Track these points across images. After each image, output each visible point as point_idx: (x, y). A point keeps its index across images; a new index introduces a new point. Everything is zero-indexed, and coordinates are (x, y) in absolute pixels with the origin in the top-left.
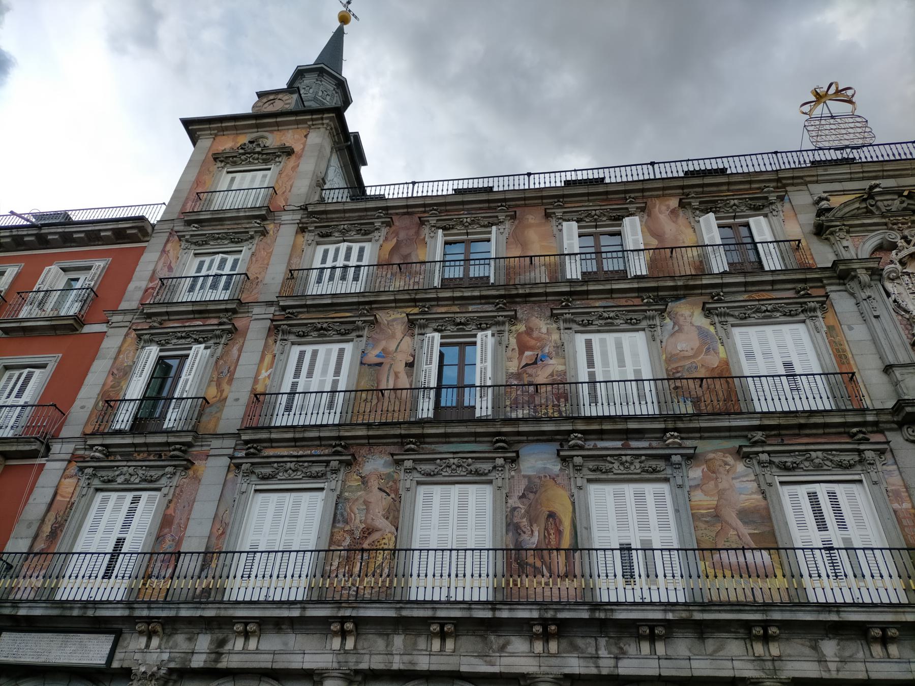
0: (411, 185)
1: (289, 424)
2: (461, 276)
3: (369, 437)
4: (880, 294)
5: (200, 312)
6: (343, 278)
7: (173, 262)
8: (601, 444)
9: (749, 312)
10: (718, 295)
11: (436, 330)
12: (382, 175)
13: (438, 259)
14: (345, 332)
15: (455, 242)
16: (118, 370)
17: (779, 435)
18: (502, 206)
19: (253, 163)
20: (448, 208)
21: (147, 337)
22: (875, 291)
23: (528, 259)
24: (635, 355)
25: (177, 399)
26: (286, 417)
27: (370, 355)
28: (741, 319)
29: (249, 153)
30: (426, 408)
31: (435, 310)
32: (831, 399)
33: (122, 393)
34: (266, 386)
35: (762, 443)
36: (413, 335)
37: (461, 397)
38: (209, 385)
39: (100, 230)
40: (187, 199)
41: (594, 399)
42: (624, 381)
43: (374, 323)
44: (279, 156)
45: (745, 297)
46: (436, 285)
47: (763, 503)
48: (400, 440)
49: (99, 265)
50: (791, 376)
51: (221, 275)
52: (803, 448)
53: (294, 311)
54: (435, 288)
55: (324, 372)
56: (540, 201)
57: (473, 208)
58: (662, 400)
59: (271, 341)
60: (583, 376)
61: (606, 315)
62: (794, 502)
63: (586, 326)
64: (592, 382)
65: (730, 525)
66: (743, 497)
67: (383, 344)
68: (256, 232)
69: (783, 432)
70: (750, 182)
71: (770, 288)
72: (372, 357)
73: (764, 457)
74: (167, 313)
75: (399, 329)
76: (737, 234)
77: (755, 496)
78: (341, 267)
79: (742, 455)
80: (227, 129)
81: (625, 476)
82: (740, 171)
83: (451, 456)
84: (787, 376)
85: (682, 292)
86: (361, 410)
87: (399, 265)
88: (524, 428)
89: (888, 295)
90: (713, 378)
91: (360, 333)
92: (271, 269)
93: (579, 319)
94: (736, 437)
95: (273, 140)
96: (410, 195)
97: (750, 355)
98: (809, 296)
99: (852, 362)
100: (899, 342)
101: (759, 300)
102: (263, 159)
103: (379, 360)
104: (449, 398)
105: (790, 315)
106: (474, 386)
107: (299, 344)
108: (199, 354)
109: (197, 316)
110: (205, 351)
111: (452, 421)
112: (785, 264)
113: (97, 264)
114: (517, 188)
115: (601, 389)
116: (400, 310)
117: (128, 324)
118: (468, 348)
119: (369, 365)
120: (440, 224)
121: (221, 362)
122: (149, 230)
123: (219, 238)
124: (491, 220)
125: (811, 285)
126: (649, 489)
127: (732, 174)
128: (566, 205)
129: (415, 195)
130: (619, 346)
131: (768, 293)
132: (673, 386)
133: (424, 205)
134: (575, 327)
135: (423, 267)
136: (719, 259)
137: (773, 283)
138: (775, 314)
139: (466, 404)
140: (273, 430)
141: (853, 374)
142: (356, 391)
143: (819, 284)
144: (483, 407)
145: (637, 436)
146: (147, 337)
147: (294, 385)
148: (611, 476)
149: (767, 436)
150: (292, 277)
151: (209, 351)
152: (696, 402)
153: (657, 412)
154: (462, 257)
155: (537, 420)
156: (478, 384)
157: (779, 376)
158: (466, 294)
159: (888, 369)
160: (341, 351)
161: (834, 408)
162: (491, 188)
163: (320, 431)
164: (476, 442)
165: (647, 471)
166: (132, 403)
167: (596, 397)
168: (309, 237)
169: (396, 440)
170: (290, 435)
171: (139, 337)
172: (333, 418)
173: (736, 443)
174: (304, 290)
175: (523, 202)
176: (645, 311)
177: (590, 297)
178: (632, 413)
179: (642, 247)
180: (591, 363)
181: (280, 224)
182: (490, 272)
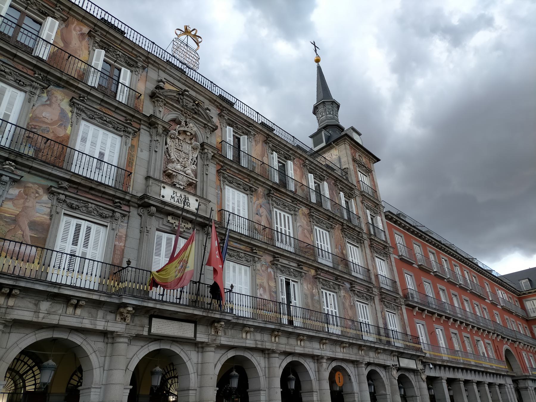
9: (96, 116)
17: (77, 188)
22: (161, 139)
28: (90, 118)
32: (114, 181)
35: (65, 189)
45: (98, 107)
47: (48, 221)
52: (86, 200)
62: (66, 227)
66: (38, 214)
69: (80, 188)
70: (133, 49)
73: (62, 197)
76: (112, 71)
77: (45, 216)
79: (50, 191)
82: (131, 39)
85: (63, 84)
89: (166, 144)
90: (55, 142)
97: (84, 140)
99: (134, 167)
100: (159, 168)
101: (104, 113)
127: (126, 37)
131: (111, 112)
136: (95, 78)
138: (109, 124)
149: (70, 187)
152: (38, 151)
157: (94, 158)
173: (49, 183)
176: (33, 81)
179: (52, 42)
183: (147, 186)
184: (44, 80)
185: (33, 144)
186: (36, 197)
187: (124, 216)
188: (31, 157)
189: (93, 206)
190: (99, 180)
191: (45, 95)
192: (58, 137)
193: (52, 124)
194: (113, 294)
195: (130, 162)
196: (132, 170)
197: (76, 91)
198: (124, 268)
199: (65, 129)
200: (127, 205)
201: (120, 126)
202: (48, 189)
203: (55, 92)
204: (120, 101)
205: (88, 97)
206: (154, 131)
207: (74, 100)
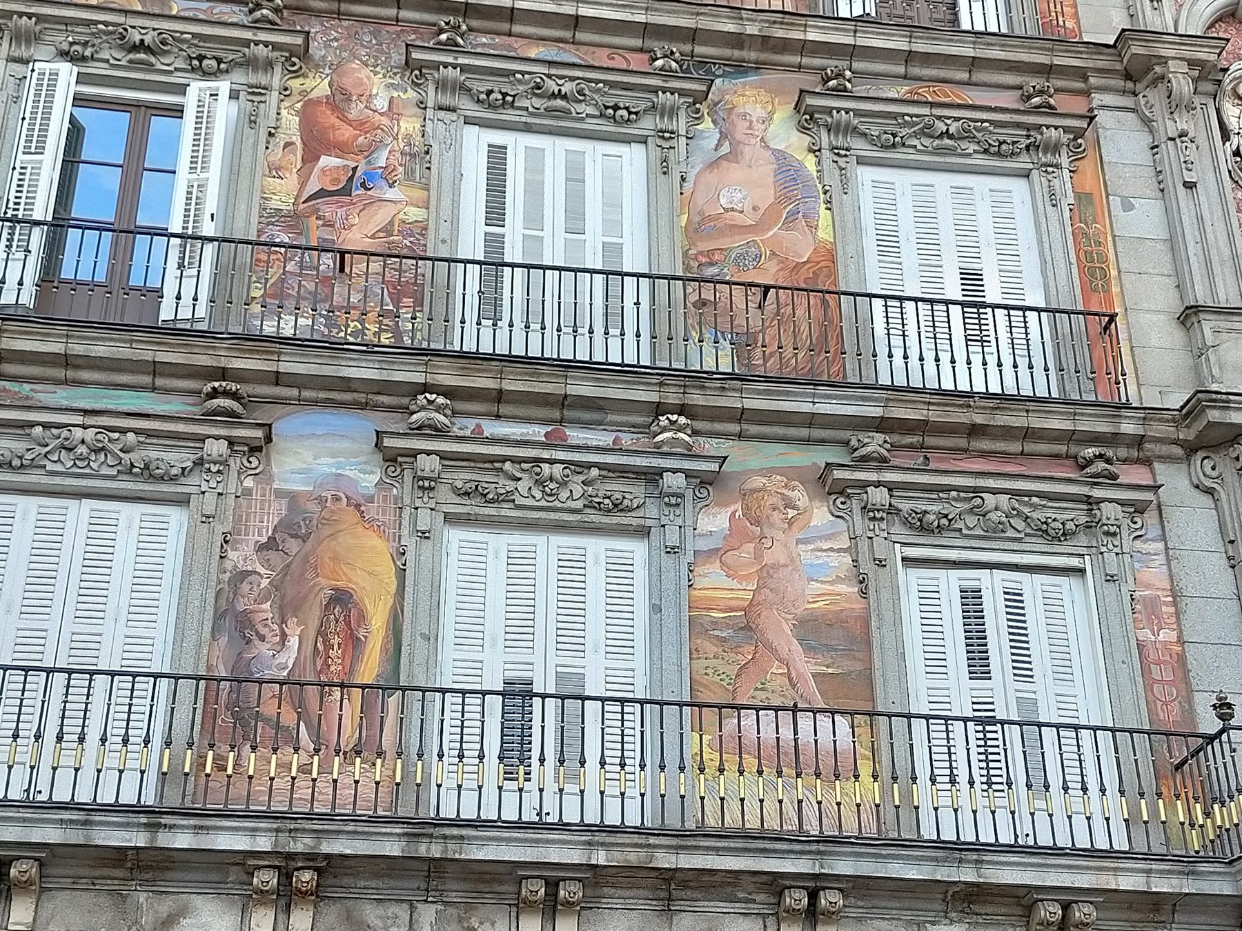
4: (1208, 130)
8: (492, 428)
9: (905, 131)
10: (840, 75)
11: (64, 55)
24: (612, 204)
37: (121, 260)
41: (491, 306)
42: (576, 270)
45: (902, 91)
50: (974, 305)
58: (663, 330)
60: (472, 245)
61: (551, 86)
63: (496, 108)
64: (493, 264)
65: (774, 652)
69: (931, 441)
71: (964, 76)
73: (879, 496)
77: (841, 588)
81: (543, 515)
84: (962, 304)
93: (479, 86)
94: (823, 442)
97: (889, 244)
98: (1050, 110)
101: (932, 105)
104: (85, 258)
105: (998, 154)
111: (88, 324)
112: (1010, 20)
115: (513, 283)
125: (1060, 84)
126: (596, 548)
130: (575, 177)
132: (694, 298)
134: (467, 106)
137: (974, 63)
139: (136, 280)
141: (1112, 318)
143: (1080, 85)
144: (185, 294)
145: (586, 416)
148: (507, 511)
149: (895, 447)
153: (645, 361)
155: (334, 347)
157: (947, 303)
159: (1189, 315)
161: (1055, 394)
164: (154, 389)
165: (598, 507)
167: (497, 303)
177: (517, 28)
178: (583, 356)
180: (496, 214)
183: (1199, 352)
184: (688, 71)
185: (724, 324)
186: (791, 522)
187: (1139, 509)
188: (732, 377)
189: (1004, 498)
190: (995, 388)
191: (707, 124)
192: (798, 266)
193: (758, 227)
194: (1198, 859)
195: (1093, 270)
196: (1112, 305)
197: (805, 61)
198: (1210, 739)
199: (813, 228)
200: (1138, 461)
201: (1009, 134)
202: (822, 479)
203: (736, 99)
204: (979, 27)
205: (856, 65)
206: (1155, 97)
207: (810, 101)
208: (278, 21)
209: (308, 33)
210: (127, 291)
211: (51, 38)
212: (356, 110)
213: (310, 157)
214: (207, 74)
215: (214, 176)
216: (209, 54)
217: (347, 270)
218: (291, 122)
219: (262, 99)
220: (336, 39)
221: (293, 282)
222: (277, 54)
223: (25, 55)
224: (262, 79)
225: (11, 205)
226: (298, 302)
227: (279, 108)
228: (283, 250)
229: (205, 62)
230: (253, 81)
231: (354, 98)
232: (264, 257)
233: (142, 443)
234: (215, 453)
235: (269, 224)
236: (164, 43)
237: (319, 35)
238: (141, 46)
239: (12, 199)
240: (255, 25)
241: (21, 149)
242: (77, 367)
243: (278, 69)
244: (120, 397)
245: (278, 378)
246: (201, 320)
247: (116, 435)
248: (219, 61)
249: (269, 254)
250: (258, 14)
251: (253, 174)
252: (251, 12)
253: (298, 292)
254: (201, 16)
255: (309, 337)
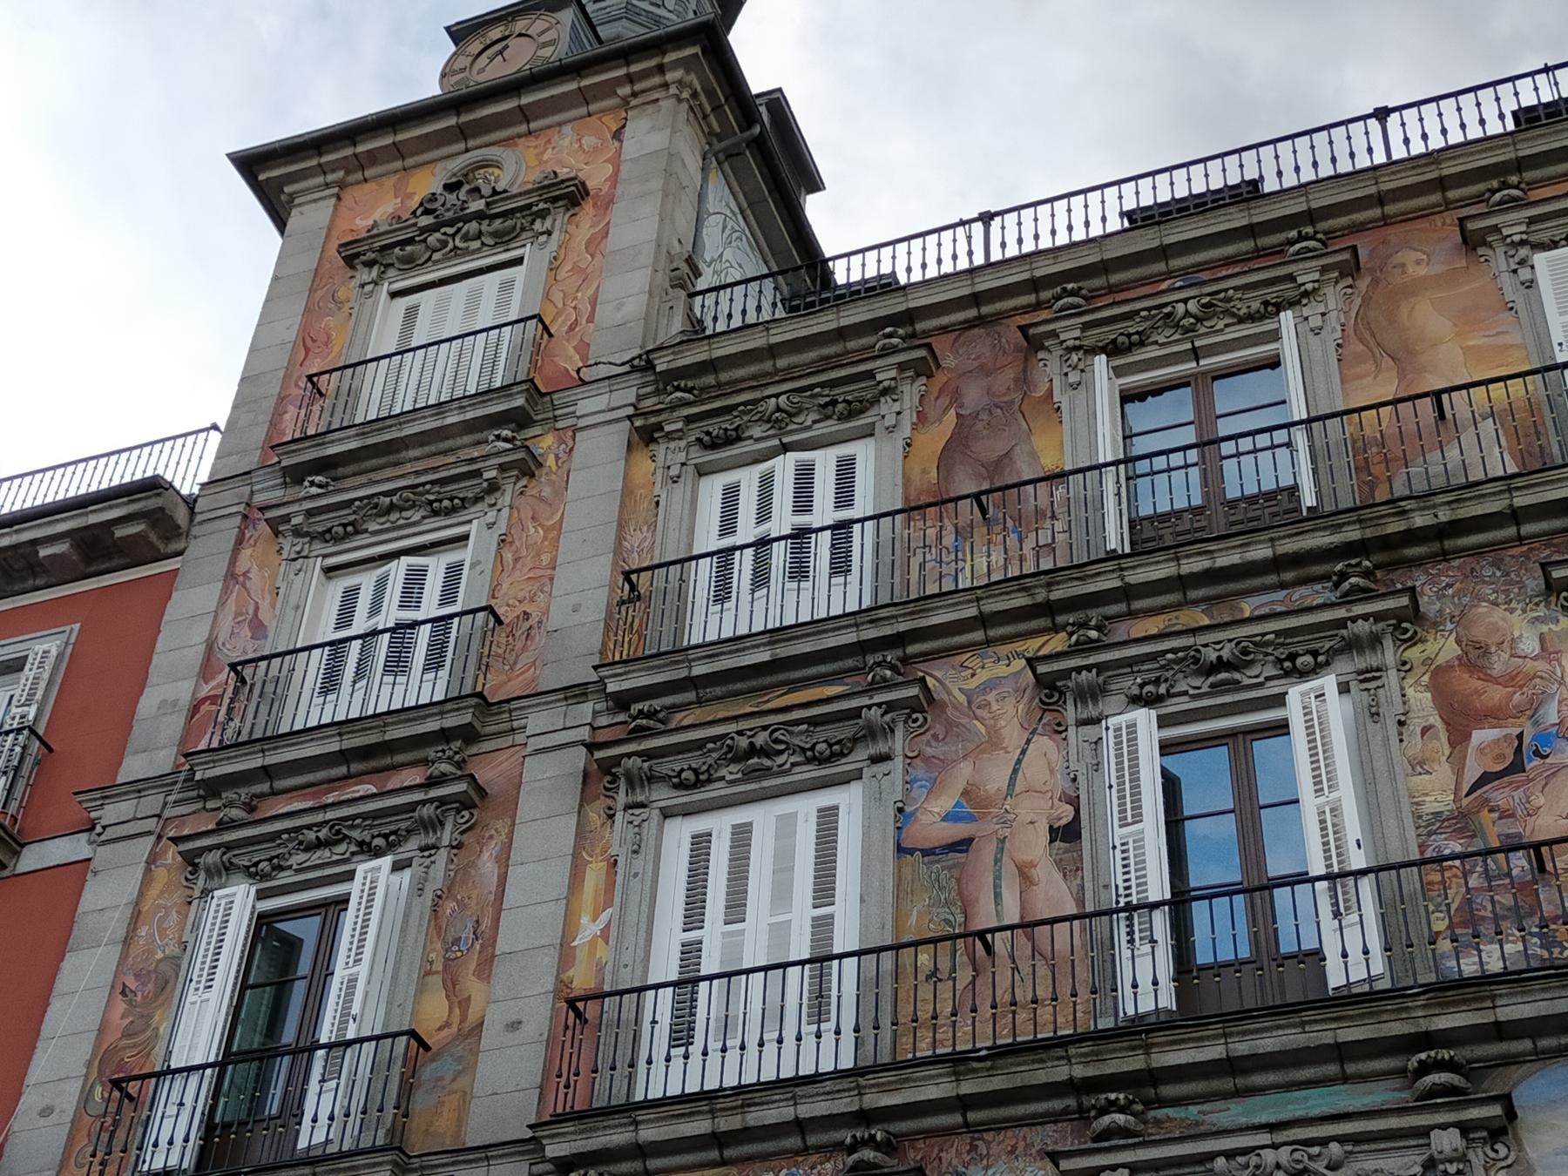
0: (978, 228)
1: (692, 1087)
2: (1197, 501)
3: (963, 1103)
5: (365, 753)
6: (799, 571)
7: (265, 606)
11: (1137, 701)
12: (879, 210)
13: (1106, 453)
14: (830, 752)
15: (1157, 390)
16: (137, 976)
18: (1302, 238)
19: (467, 252)
20: (1115, 278)
21: (212, 858)
23: (1426, 405)
25: (329, 1046)
26: (678, 1063)
27: (924, 818)
29: (450, 223)
30: (1146, 979)
31: (1121, 631)
33: (160, 1051)
34: (600, 968)
36: (1059, 729)
37: (1263, 923)
38: (421, 990)
39: (35, 543)
40: (282, 399)
43: (923, 706)
44: (543, 214)
46: (1113, 544)
48: (1071, 1102)
49: (45, 649)
51: (415, 624)
53: (657, 703)
54: (1113, 556)
55: (782, 895)
56: (1435, 198)
57: (1198, 267)
59: (595, 815)
67: (965, 770)
68: (502, 468)
72: (932, 823)
74: (267, 772)
75: (1010, 714)
78: (790, 536)
80: (373, 158)
83: (1264, 1138)
86: (925, 1013)
87: (977, 497)
88: (1515, 1009)
91: (881, 747)
92: (565, 579)
95: (516, 167)
96: (979, 260)
102: (494, 234)
103: (959, 831)
104: (1220, 933)
106: (1303, 878)
107: (688, 812)
108: (378, 887)
109: (356, 767)
110: (396, 878)
111: (1245, 1015)
113: (39, 648)
114: (1344, 166)
116: (1003, 650)
117: (151, 824)
118: (1261, 747)
119: (926, 852)
120: (1094, 337)
121: (449, 906)
122: (181, 516)
123: (392, 508)
124: (1271, 293)
128: (1535, 195)
129: (996, 256)
133: (1034, 285)
135: (1060, 492)
139: (1287, 946)
140: (642, 1116)
142: (896, 947)
144: (1352, 950)
146: (212, 858)
147: (691, 952)
150: (635, 596)
151: (406, 875)
154: (1188, 436)
156: (1318, 869)
158: (1223, 561)
160: (828, 818)
162: (1255, 184)
163: (795, 1101)
164: (1345, 1079)
166: (194, 1079)
168: (670, 454)
169: (1057, 1104)
170: (699, 1126)
171: (191, 860)
172: (832, 1052)
174: (678, 632)
175: (1376, 212)
181: (576, 430)
182: (1296, 470)
208: (1373, 586)
209: (1413, 589)
210: (1280, 961)
211: (1118, 686)
212: (1499, 663)
213: (1459, 737)
214: (1304, 674)
215: (1347, 793)
216: (1300, 650)
217: (1549, 867)
218: (1421, 701)
219: (1379, 683)
220: (1451, 586)
221: (1483, 900)
222: (1381, 625)
223: (1095, 714)
224: (1372, 660)
225: (1121, 891)
226: (1497, 925)
227: (1402, 689)
228: (1457, 863)
229: (1299, 661)
230: (1363, 666)
231: (1493, 649)
232: (1437, 877)
233: (1351, 1153)
234: (1447, 1148)
235: (1430, 834)
236: (1245, 652)
237: (1427, 588)
238: (1221, 665)
239: (1121, 885)
240: (1347, 599)
241: (1116, 823)
242: (1246, 1072)
243: (1388, 642)
244: (1306, 1099)
245: (1500, 1031)
246: (1380, 977)
247: (1315, 1150)
248: (1315, 654)
249: (1442, 871)
250: (1346, 586)
251: (1393, 779)
252: (1337, 585)
253: (1493, 912)
254: (1280, 609)
255: (1524, 967)
